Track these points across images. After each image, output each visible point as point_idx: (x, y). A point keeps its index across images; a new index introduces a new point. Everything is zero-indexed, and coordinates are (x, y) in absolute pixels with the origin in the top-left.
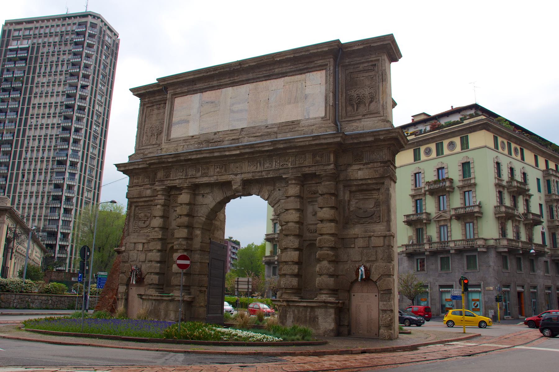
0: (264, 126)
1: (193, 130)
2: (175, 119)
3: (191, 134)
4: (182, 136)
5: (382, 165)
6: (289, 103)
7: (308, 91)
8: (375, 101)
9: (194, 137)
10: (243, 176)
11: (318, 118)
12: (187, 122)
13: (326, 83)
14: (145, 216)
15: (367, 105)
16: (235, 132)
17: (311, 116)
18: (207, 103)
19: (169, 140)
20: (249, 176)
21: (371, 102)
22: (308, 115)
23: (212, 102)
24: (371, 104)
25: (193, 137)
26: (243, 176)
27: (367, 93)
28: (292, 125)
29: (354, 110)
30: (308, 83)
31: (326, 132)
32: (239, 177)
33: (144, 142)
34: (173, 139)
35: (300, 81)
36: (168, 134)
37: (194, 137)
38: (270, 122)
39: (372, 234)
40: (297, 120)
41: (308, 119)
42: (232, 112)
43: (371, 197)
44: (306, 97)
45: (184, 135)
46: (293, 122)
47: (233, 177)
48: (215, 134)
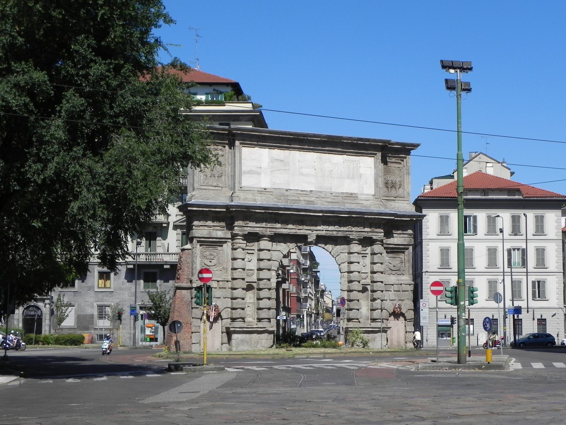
0: (329, 192)
1: (265, 182)
2: (243, 168)
3: (264, 186)
4: (254, 186)
5: (409, 236)
6: (348, 178)
7: (362, 171)
8: (402, 187)
9: (267, 190)
10: (318, 232)
11: (370, 195)
12: (259, 174)
13: (375, 168)
14: (211, 255)
15: (397, 190)
16: (304, 193)
17: (365, 192)
18: (276, 160)
19: (241, 188)
20: (323, 233)
21: (399, 188)
22: (363, 191)
23: (281, 161)
24: (400, 189)
25: (265, 189)
26: (318, 232)
27: (398, 180)
28: (352, 196)
29: (389, 191)
30: (362, 165)
31: (379, 208)
32: (315, 232)
33: (202, 181)
34: (244, 187)
35: (356, 161)
36: (240, 183)
37: (267, 190)
38: (333, 190)
39: (403, 282)
40: (354, 193)
41: (362, 194)
42: (302, 174)
43: (398, 256)
44: (361, 176)
45: (256, 186)
46: (351, 194)
47: (310, 232)
48: (287, 190)
